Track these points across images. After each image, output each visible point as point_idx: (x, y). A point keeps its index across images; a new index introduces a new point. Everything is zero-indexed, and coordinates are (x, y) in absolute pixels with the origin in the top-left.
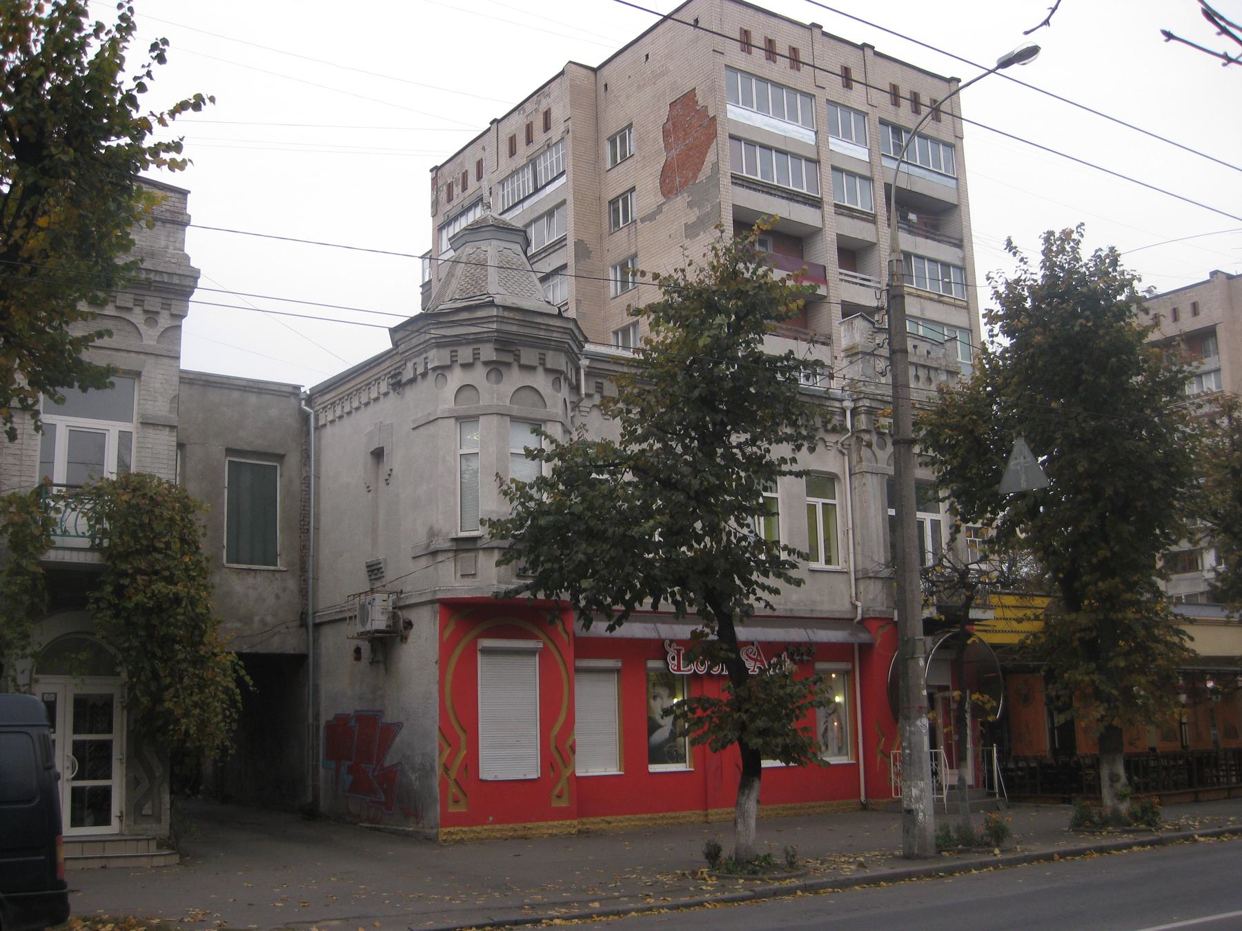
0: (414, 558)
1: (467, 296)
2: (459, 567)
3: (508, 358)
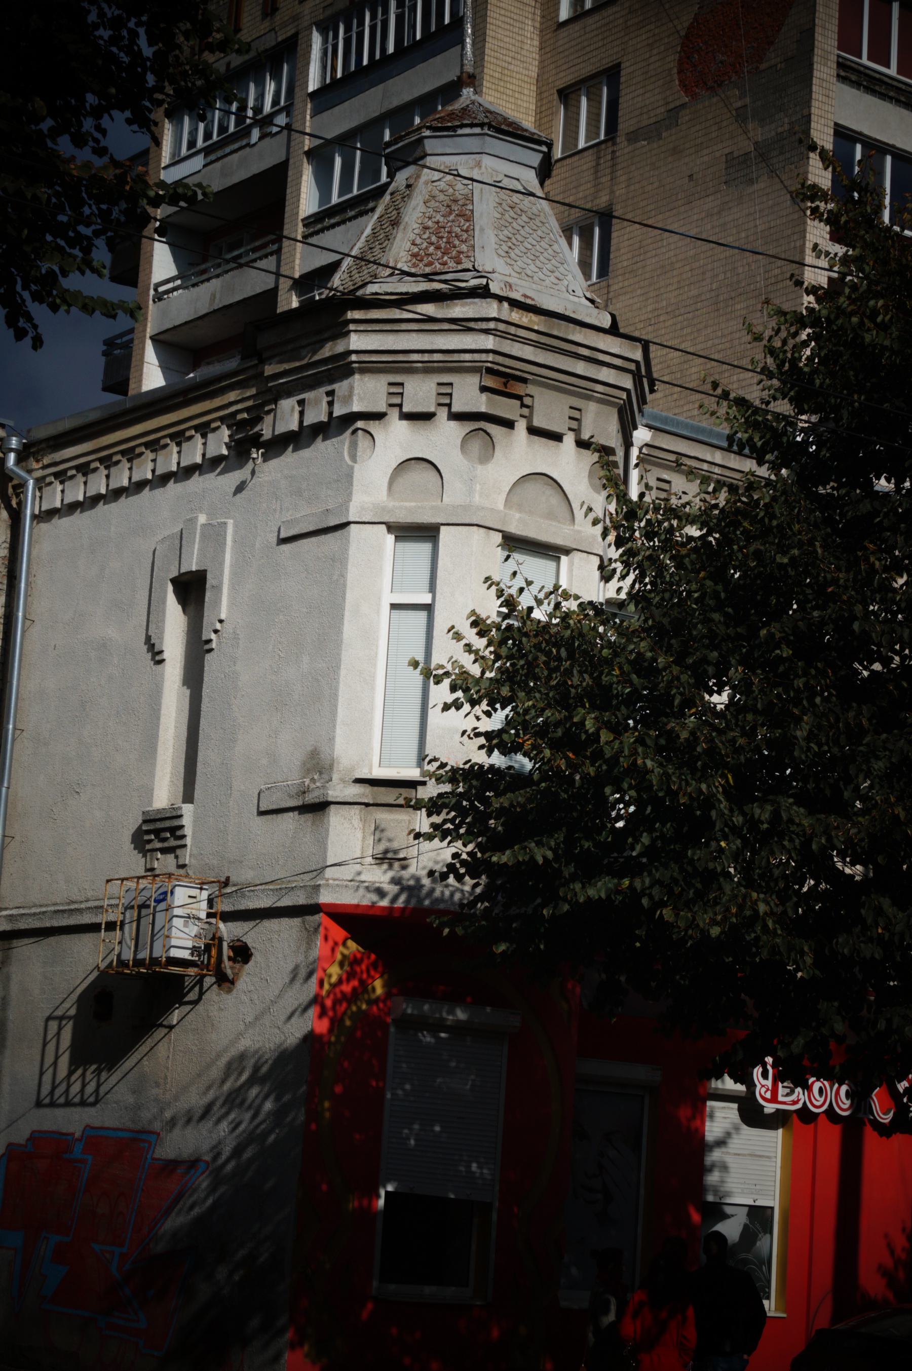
1: (428, 270)
3: (506, 408)
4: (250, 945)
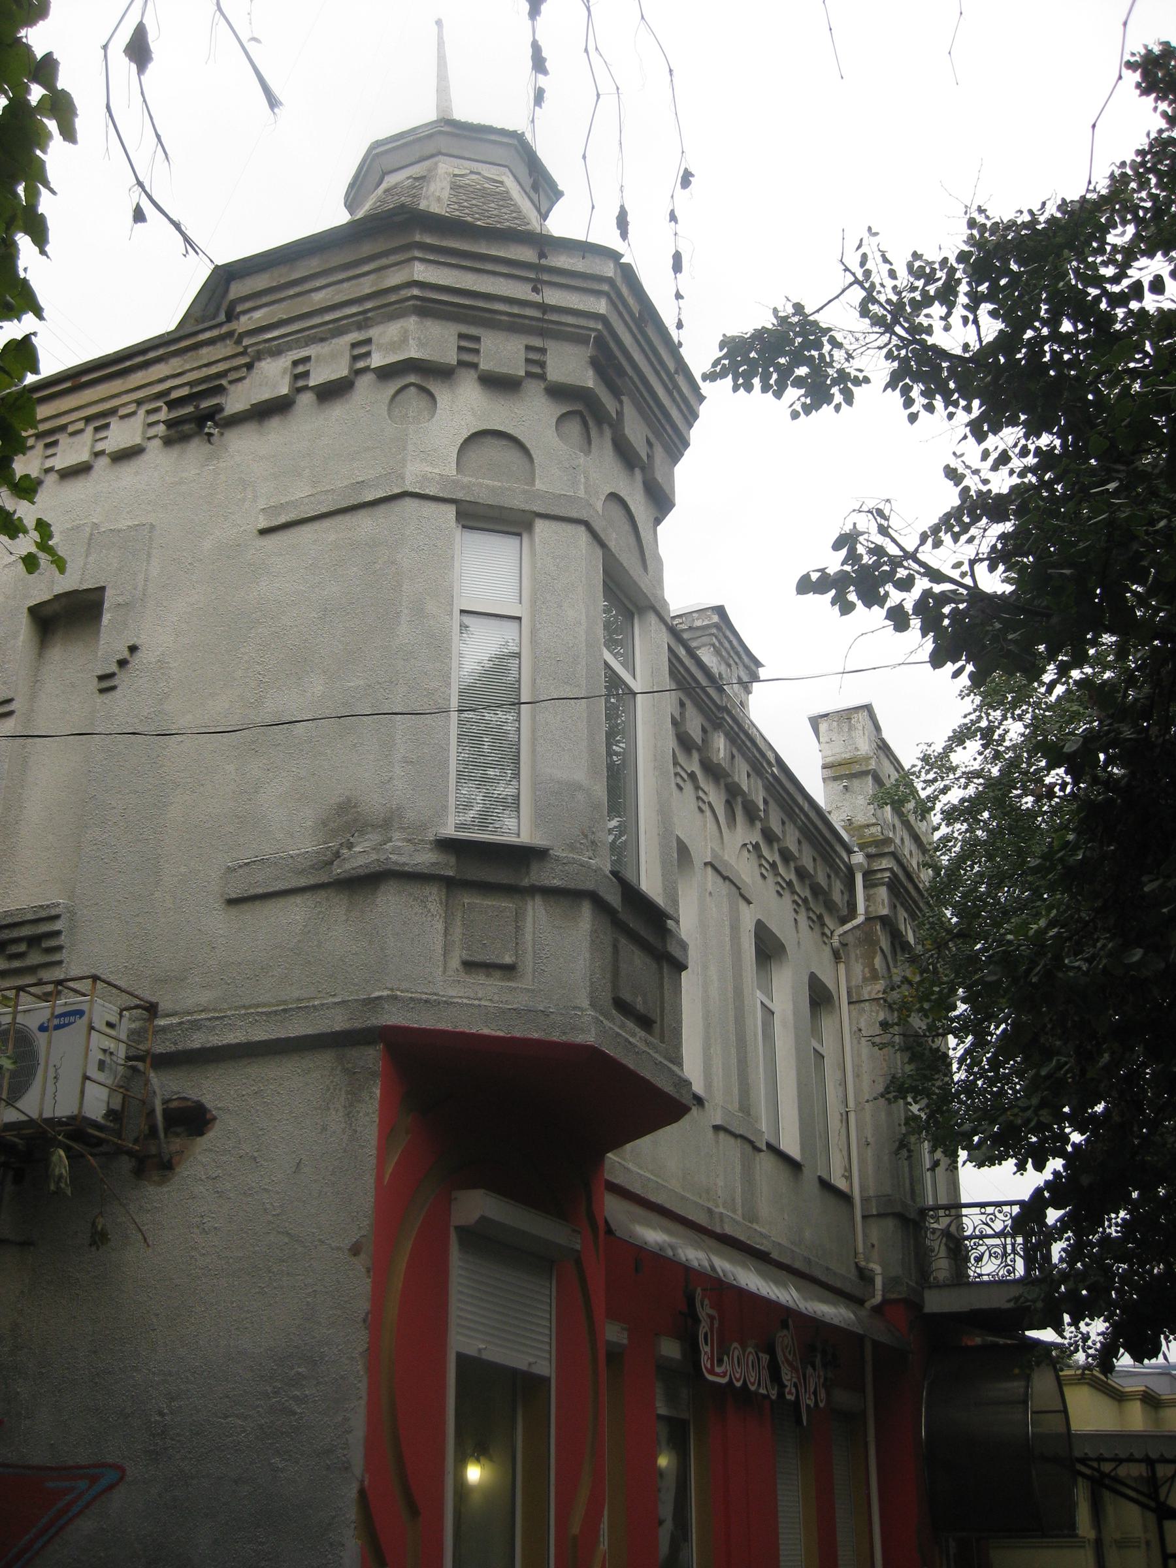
0: (232, 902)
2: (457, 932)
4: (209, 1106)
